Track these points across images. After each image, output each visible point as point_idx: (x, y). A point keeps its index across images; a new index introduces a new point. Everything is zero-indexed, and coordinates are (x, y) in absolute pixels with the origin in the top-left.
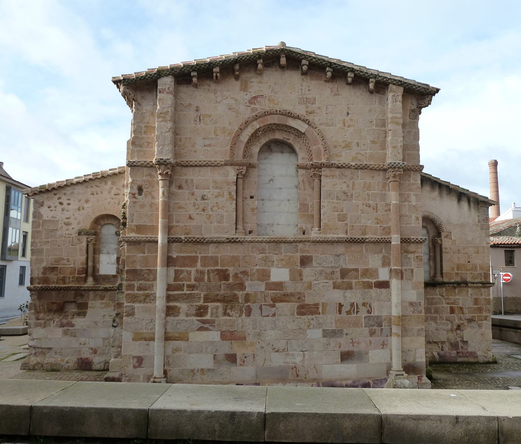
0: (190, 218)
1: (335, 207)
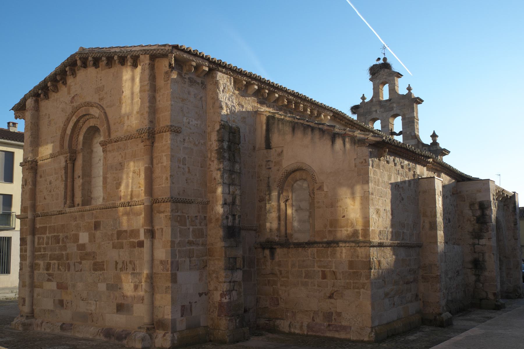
0: (45, 199)
1: (114, 177)
